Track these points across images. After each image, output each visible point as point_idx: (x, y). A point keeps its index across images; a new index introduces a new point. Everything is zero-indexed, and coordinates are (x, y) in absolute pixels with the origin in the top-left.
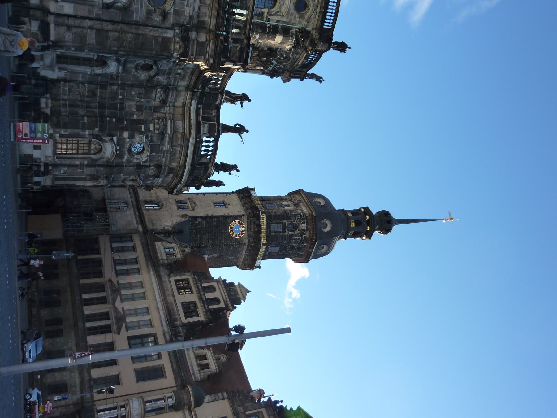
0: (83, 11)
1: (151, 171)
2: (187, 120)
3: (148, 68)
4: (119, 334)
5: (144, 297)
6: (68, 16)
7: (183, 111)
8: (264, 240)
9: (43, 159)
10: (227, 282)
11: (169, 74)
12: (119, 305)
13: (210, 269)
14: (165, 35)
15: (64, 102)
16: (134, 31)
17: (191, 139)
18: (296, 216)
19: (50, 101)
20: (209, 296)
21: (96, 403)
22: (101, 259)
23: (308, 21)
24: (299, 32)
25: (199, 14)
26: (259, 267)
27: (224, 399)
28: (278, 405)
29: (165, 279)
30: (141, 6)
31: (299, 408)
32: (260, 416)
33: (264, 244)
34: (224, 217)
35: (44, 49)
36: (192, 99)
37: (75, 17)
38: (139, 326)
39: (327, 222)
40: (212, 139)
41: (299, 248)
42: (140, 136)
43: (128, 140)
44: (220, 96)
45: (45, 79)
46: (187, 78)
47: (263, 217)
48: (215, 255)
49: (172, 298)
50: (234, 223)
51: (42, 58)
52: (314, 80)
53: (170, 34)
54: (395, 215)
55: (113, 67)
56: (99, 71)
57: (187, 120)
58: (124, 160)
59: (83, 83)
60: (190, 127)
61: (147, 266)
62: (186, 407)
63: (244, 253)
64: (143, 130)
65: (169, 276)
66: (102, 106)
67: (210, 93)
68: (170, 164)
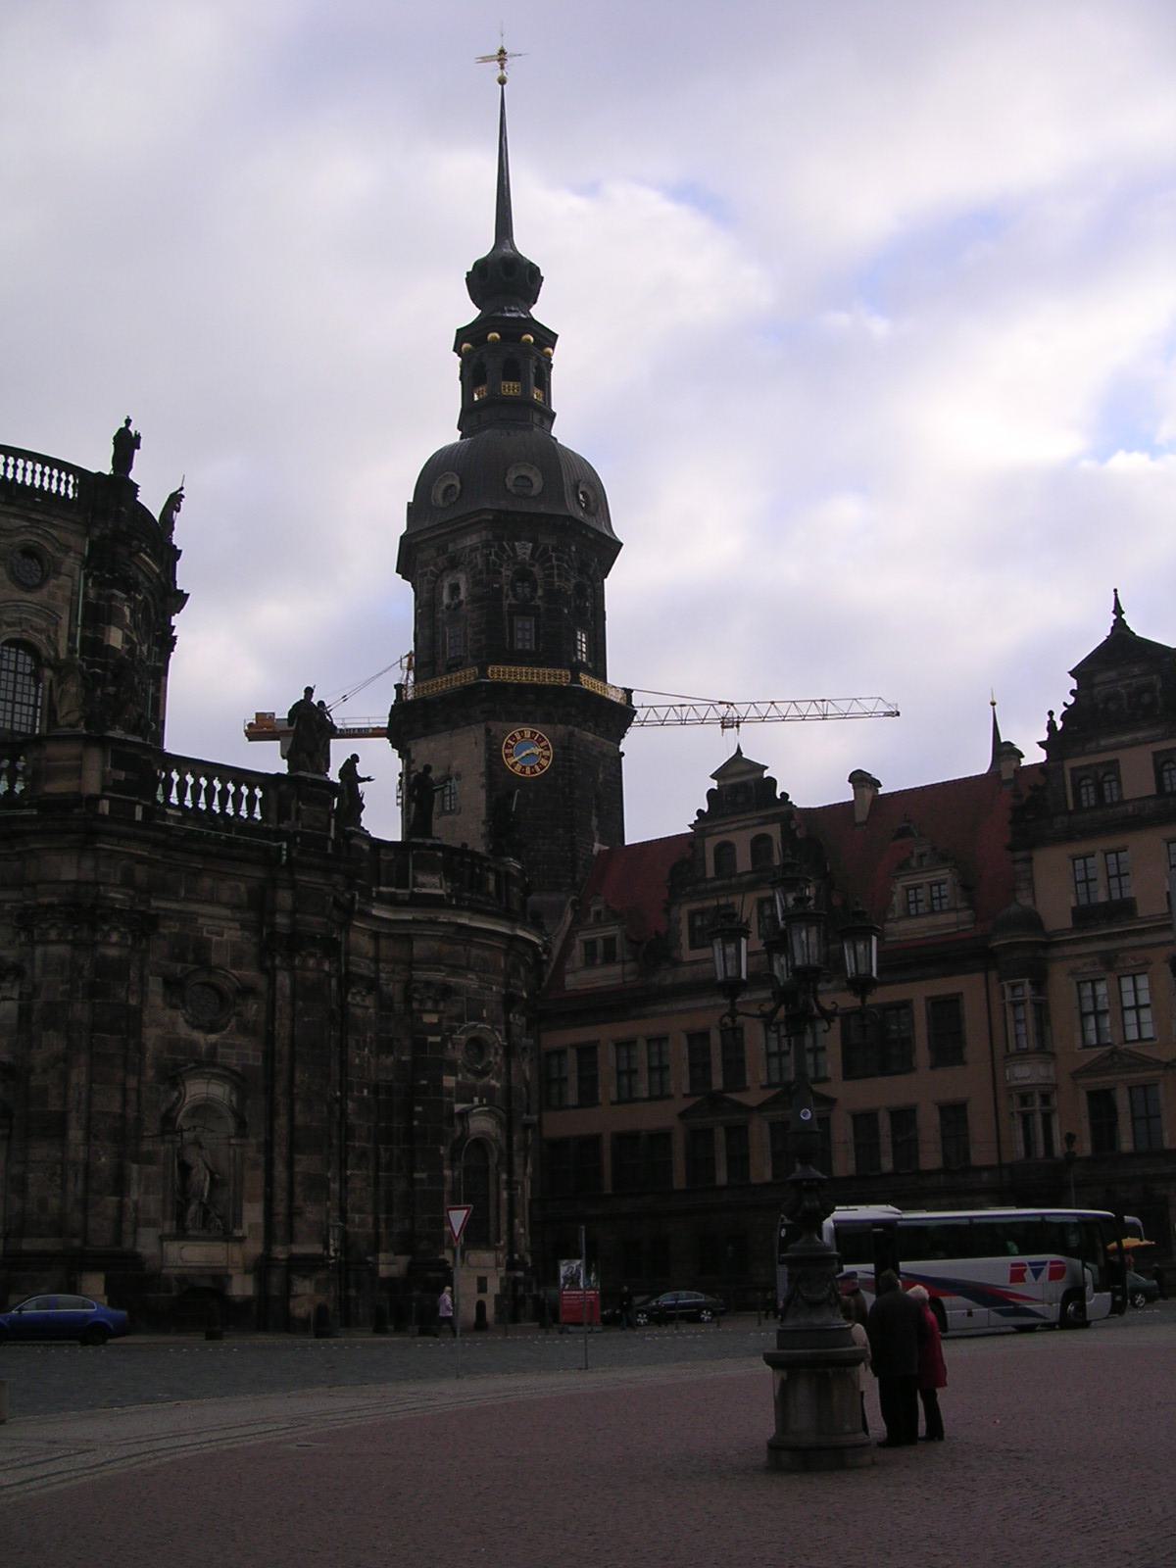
0: (254, 1180)
4: (831, 1102)
6: (269, 1213)
7: (390, 936)
8: (561, 677)
10: (706, 810)
13: (630, 839)
14: (288, 991)
15: (383, 1225)
19: (382, 1256)
20: (744, 862)
21: (1006, 1160)
23: (67, 549)
24: (95, 578)
25: (235, 907)
26: (628, 692)
27: (1029, 860)
28: (1059, 725)
29: (685, 974)
30: (232, 1046)
31: (1073, 673)
33: (576, 679)
34: (491, 786)
37: (269, 1200)
39: (512, 475)
42: (450, 1046)
43: (460, 1076)
44: (354, 841)
47: (498, 673)
48: (595, 822)
52: (179, 518)
54: (483, 244)
59: (345, 1181)
63: (590, 736)
64: (438, 1039)
65: (677, 963)
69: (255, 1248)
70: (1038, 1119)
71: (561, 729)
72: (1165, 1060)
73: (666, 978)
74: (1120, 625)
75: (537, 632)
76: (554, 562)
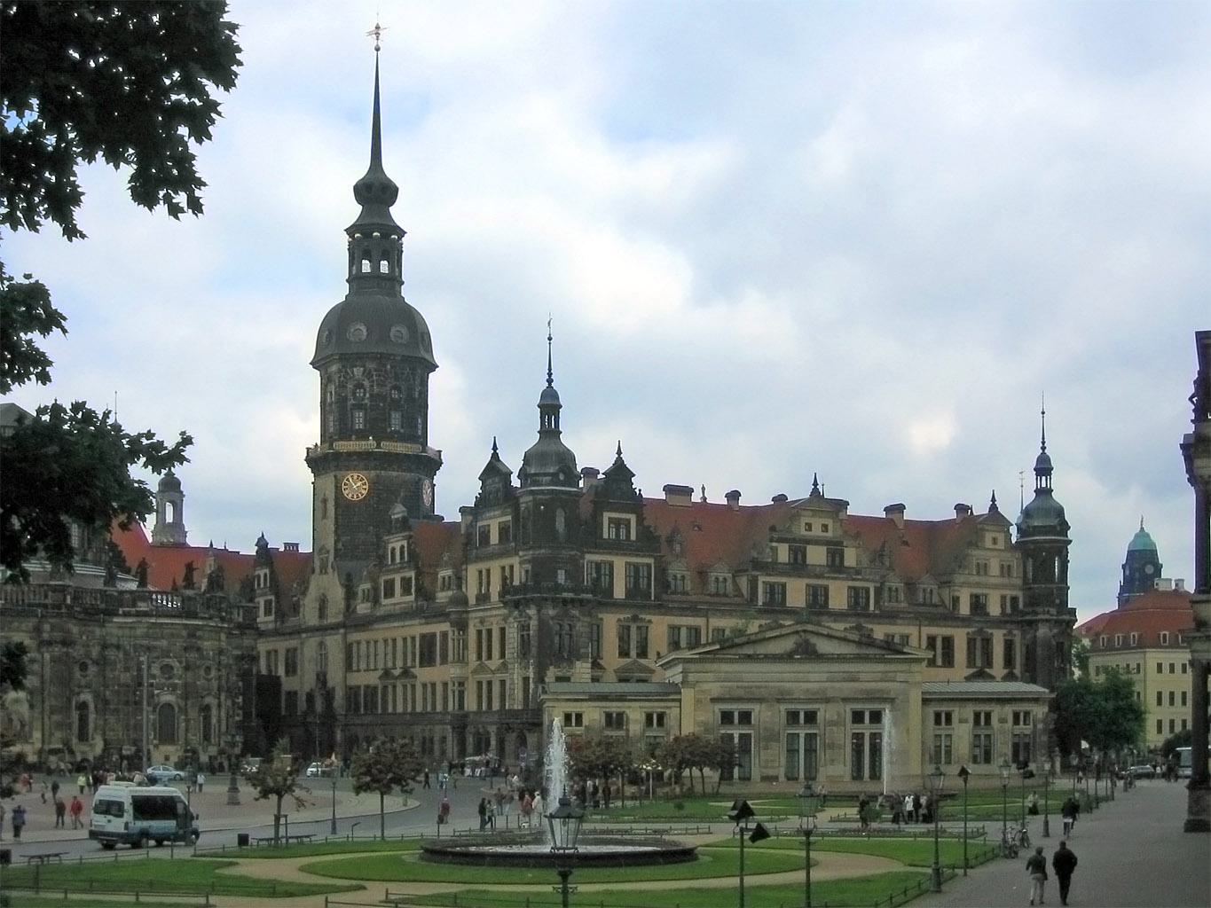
0: (37, 724)
1: (193, 656)
2: (136, 625)
3: (84, 667)
5: (394, 640)
6: (43, 735)
8: (370, 444)
9: (181, 753)
11: (88, 646)
12: (397, 672)
16: (48, 685)
17: (151, 621)
18: (342, 386)
20: (398, 560)
22: (365, 686)
27: (466, 570)
32: (482, 530)
33: (378, 446)
34: (337, 506)
35: (72, 752)
36: (112, 622)
37: (43, 730)
38: (414, 654)
40: (154, 597)
41: (396, 377)
43: (157, 680)
45: (104, 750)
46: (90, 629)
49: (397, 607)
50: (347, 492)
51: (83, 753)
53: (47, 656)
55: (86, 697)
56: (92, 707)
57: (136, 625)
58: (180, 682)
60: (140, 622)
61: (372, 630)
62: (464, 616)
63: (395, 474)
65: (380, 604)
66: (127, 703)
67: (107, 602)
68: (183, 637)
69: (38, 745)
70: (456, 694)
71: (373, 473)
72: (493, 669)
73: (380, 612)
74: (495, 456)
75: (365, 420)
76: (375, 378)
